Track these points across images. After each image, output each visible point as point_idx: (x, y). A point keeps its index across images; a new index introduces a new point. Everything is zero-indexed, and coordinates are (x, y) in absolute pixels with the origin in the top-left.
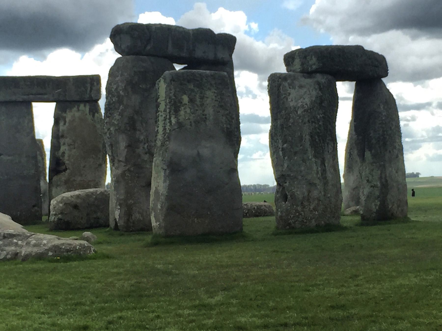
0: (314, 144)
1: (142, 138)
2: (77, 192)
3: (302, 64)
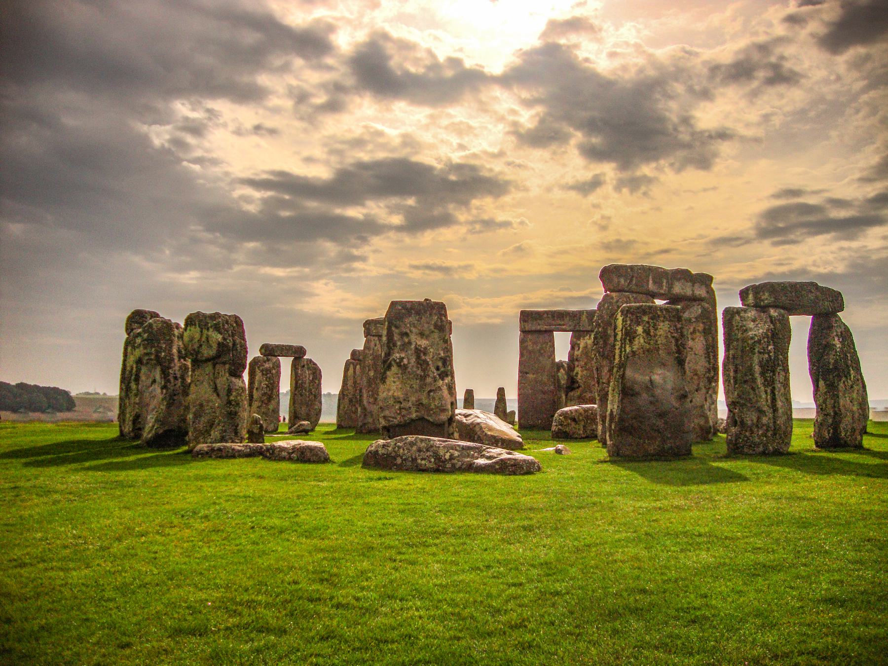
0: (762, 374)
3: (755, 298)
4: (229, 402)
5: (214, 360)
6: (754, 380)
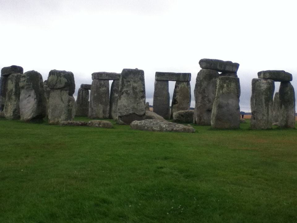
0: (265, 102)
1: (206, 96)
2: (183, 111)
4: (69, 105)
5: (61, 89)
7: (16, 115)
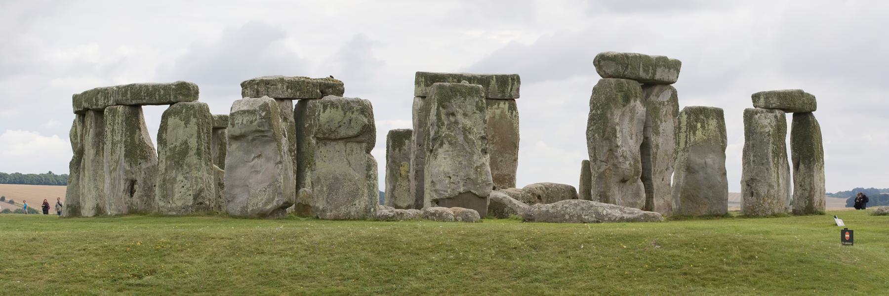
3: (766, 102)
5: (347, 139)
6: (768, 163)
7: (201, 203)
